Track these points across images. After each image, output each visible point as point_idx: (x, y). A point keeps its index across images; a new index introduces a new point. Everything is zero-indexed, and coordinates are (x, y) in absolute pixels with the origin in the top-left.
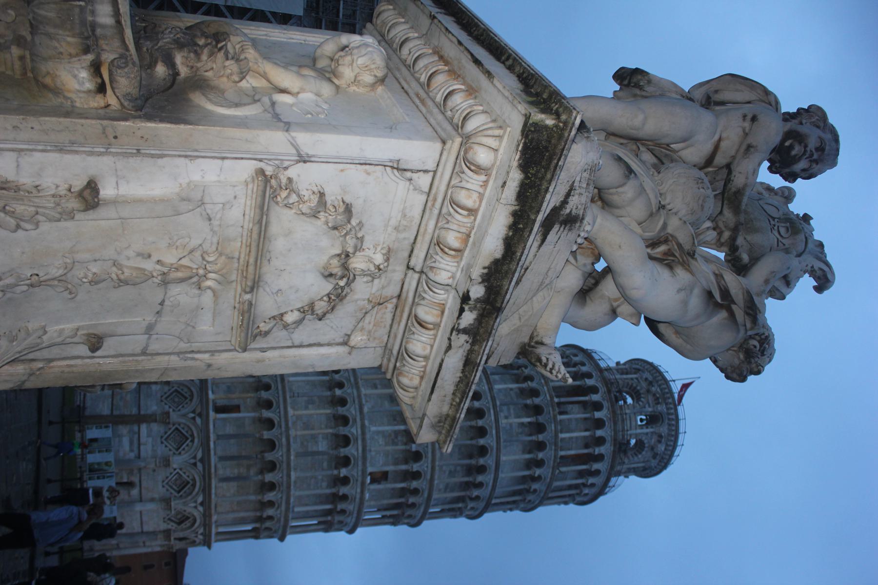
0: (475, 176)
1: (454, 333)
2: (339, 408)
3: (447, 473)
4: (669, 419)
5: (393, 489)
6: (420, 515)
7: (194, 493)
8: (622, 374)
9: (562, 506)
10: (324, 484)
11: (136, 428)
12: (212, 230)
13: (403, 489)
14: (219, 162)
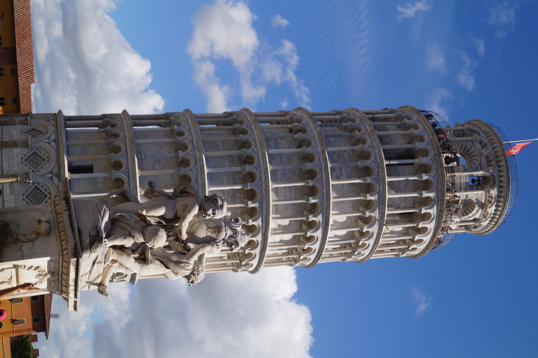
2: (182, 169)
4: (500, 181)
8: (458, 136)
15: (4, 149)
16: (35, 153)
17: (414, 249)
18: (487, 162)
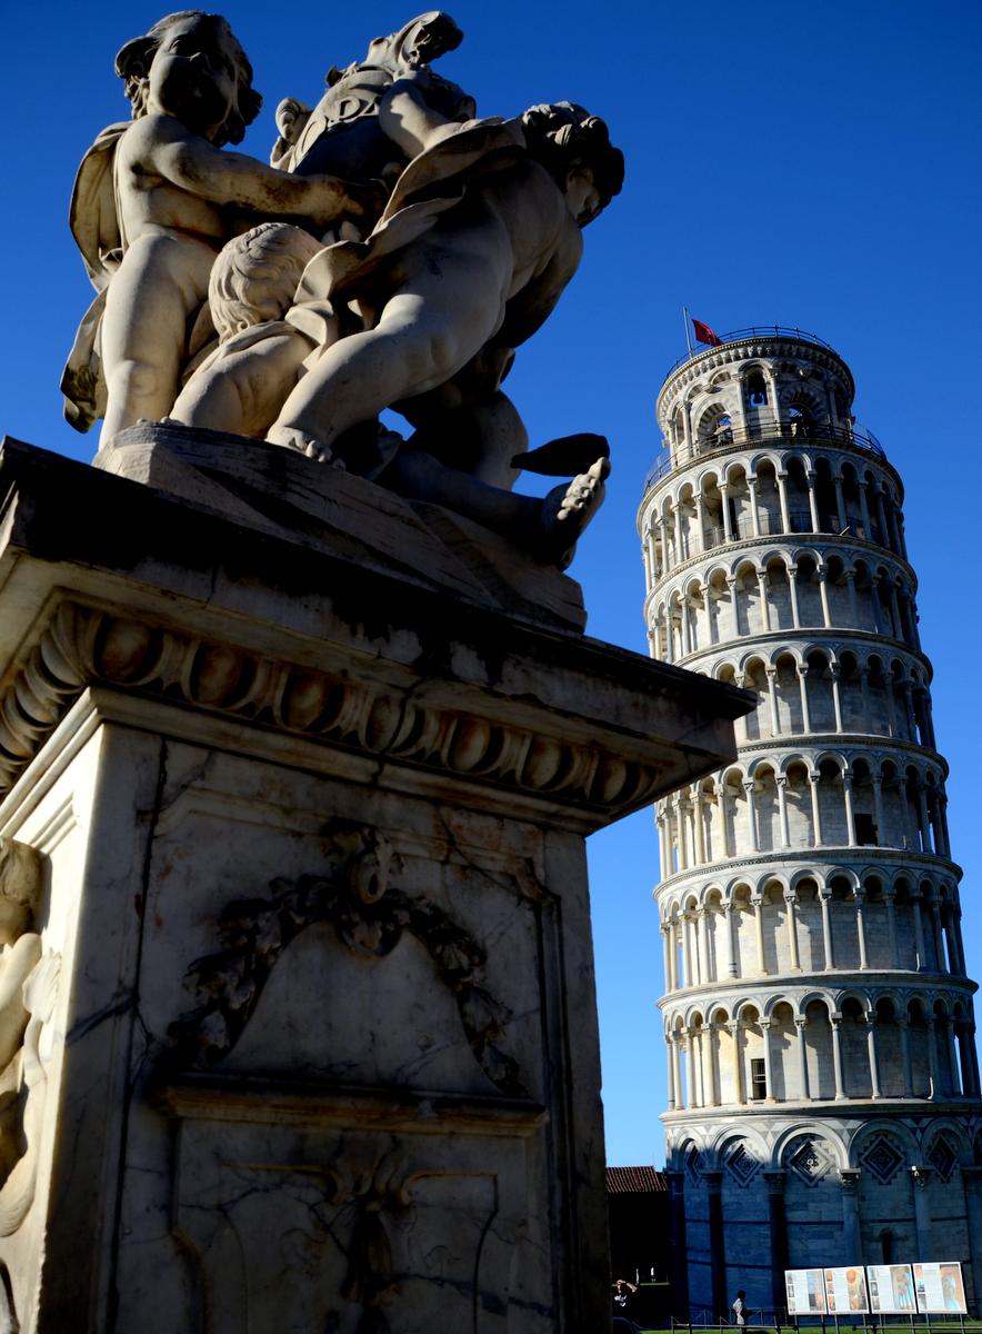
0: (165, 656)
1: (498, 688)
3: (854, 717)
4: (755, 354)
5: (885, 806)
6: (926, 759)
9: (905, 524)
10: (880, 918)
11: (794, 1229)
12: (278, 1186)
13: (884, 790)
14: (130, 1175)
15: (725, 1218)
17: (885, 486)
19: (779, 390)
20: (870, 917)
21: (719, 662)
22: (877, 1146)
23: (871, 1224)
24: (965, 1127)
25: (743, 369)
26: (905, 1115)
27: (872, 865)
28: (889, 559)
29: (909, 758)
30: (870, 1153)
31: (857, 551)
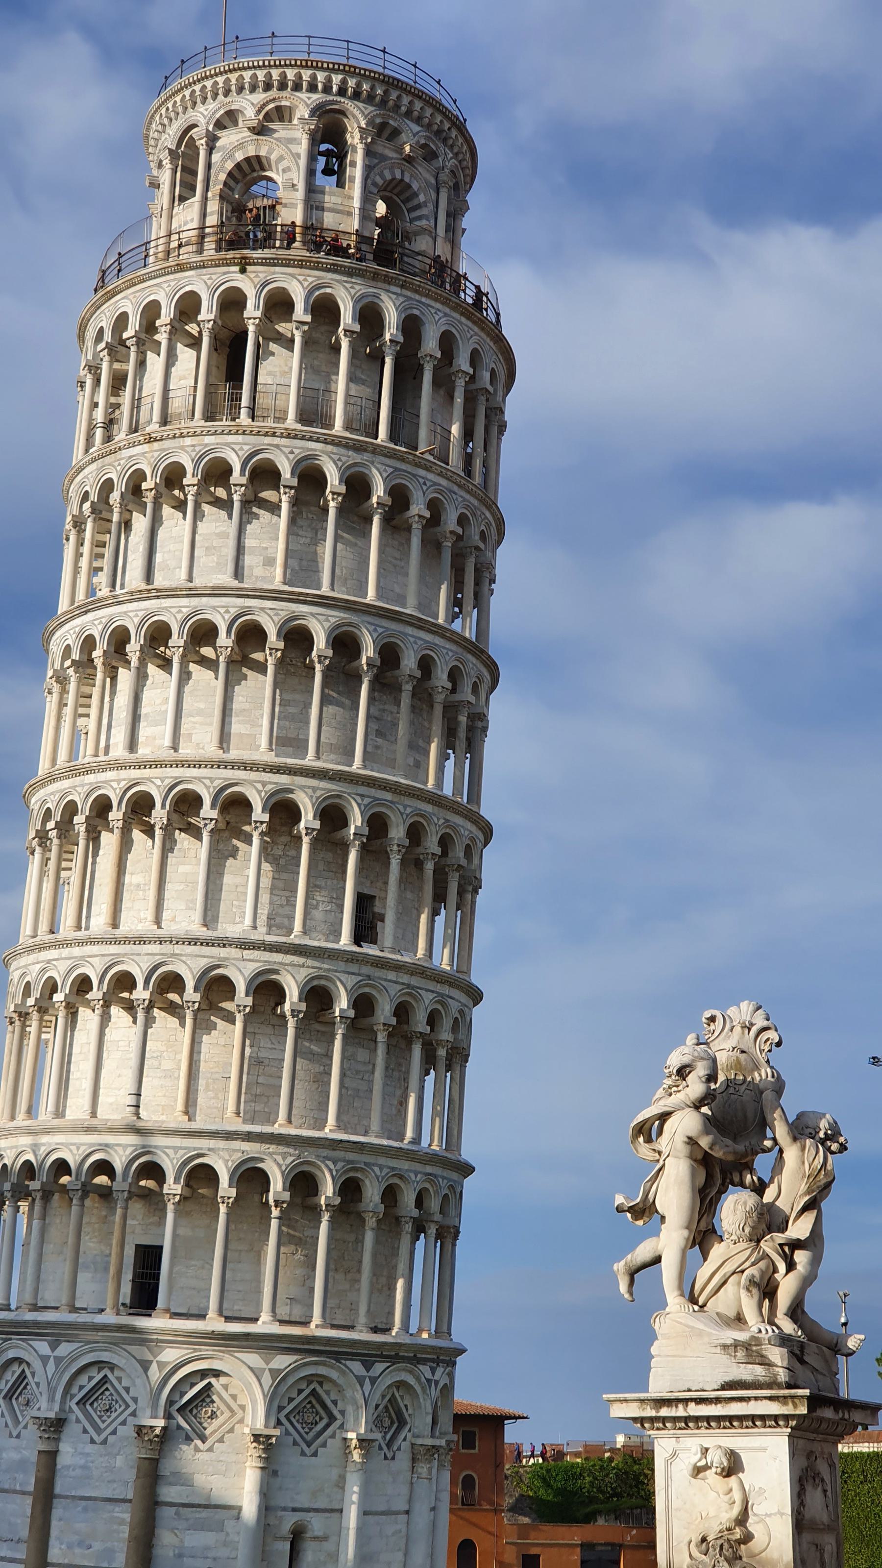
3: (379, 740)
4: (342, 92)
6: (469, 825)
7: (341, 1381)
10: (362, 1055)
11: (165, 1514)
13: (403, 863)
16: (81, 1403)
18: (281, 119)
19: (368, 169)
20: (351, 1050)
21: (195, 613)
22: (306, 1398)
23: (280, 1513)
24: (428, 1381)
25: (319, 111)
26: (352, 1356)
27: (369, 977)
28: (476, 502)
29: (447, 821)
30: (295, 1408)
31: (435, 484)
